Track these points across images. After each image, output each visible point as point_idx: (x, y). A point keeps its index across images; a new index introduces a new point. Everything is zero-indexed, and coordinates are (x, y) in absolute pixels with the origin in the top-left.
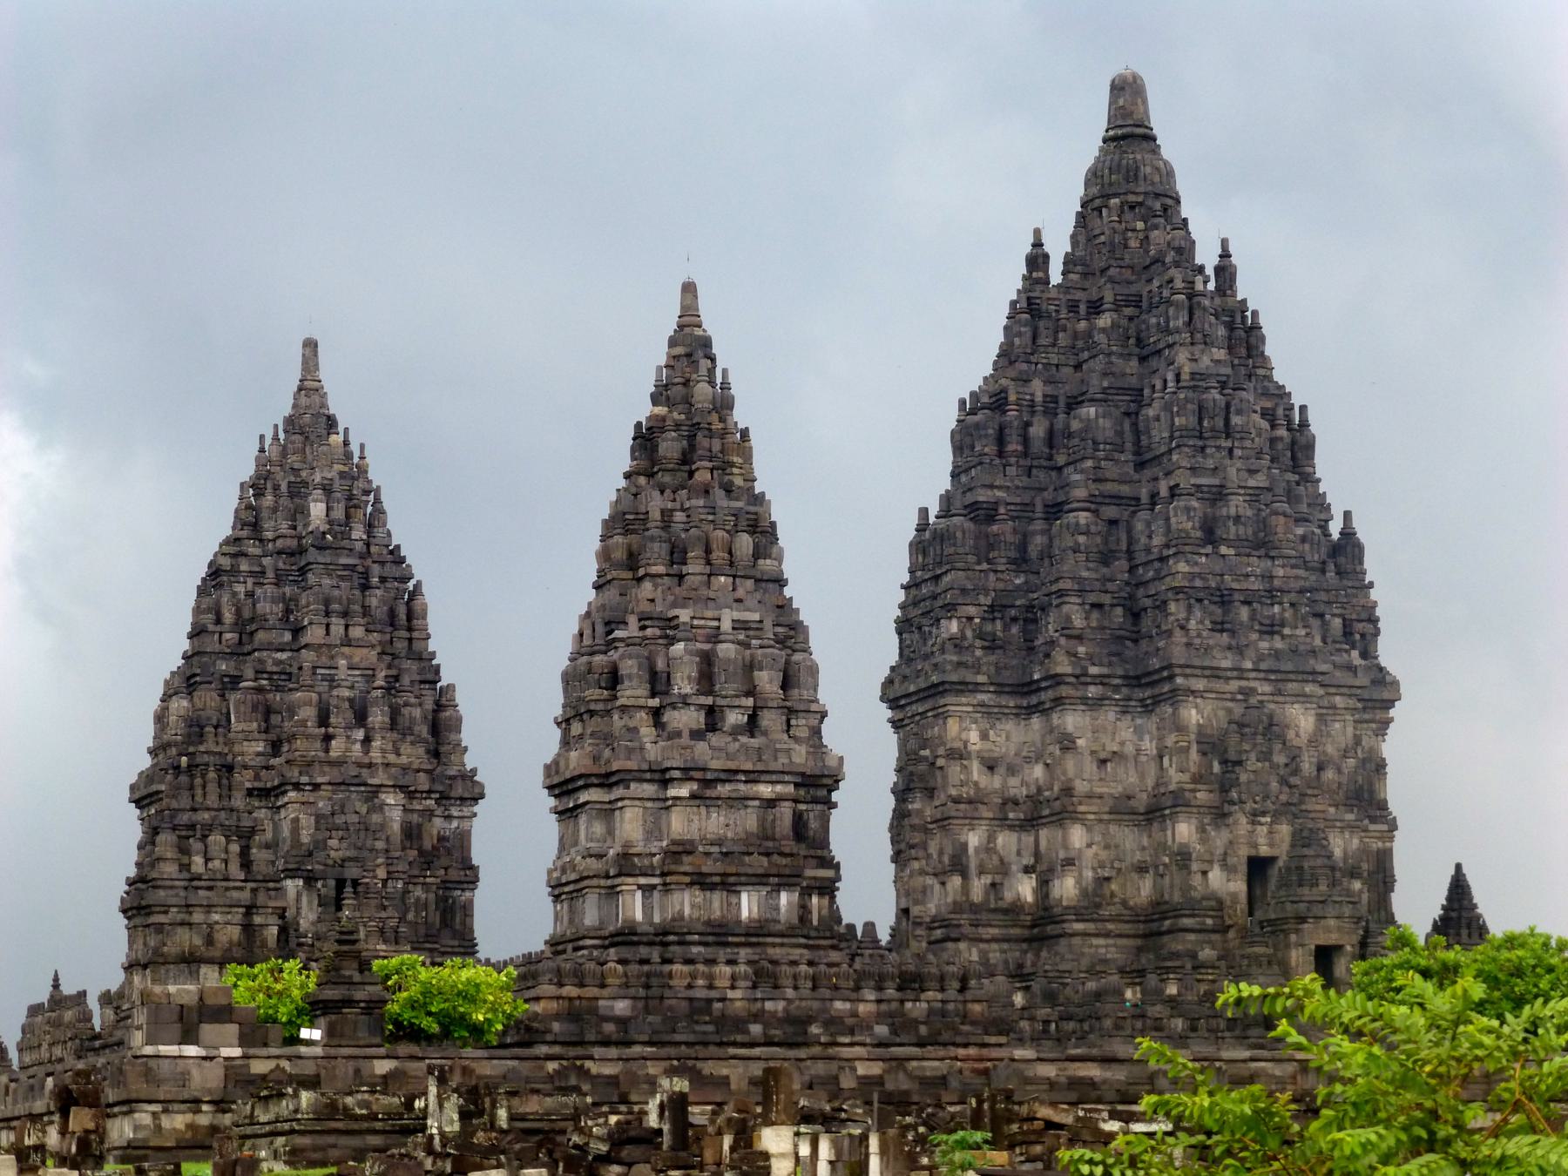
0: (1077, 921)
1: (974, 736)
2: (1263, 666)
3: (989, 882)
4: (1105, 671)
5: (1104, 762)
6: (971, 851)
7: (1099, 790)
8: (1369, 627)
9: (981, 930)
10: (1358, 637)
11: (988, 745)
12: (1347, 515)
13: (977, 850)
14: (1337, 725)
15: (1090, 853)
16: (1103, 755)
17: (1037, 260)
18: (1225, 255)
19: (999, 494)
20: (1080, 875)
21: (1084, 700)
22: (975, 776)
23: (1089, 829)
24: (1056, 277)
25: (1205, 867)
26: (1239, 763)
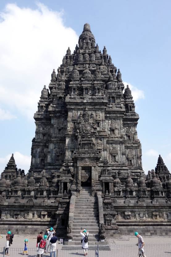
0: (49, 166)
1: (41, 129)
2: (89, 101)
3: (41, 159)
4: (60, 110)
5: (60, 130)
6: (38, 152)
7: (57, 136)
9: (37, 169)
10: (129, 107)
11: (44, 131)
13: (39, 152)
15: (55, 150)
16: (59, 128)
17: (69, 51)
18: (105, 48)
20: (52, 155)
21: (56, 117)
22: (41, 137)
23: (55, 145)
24: (72, 53)
25: (73, 150)
26: (80, 123)
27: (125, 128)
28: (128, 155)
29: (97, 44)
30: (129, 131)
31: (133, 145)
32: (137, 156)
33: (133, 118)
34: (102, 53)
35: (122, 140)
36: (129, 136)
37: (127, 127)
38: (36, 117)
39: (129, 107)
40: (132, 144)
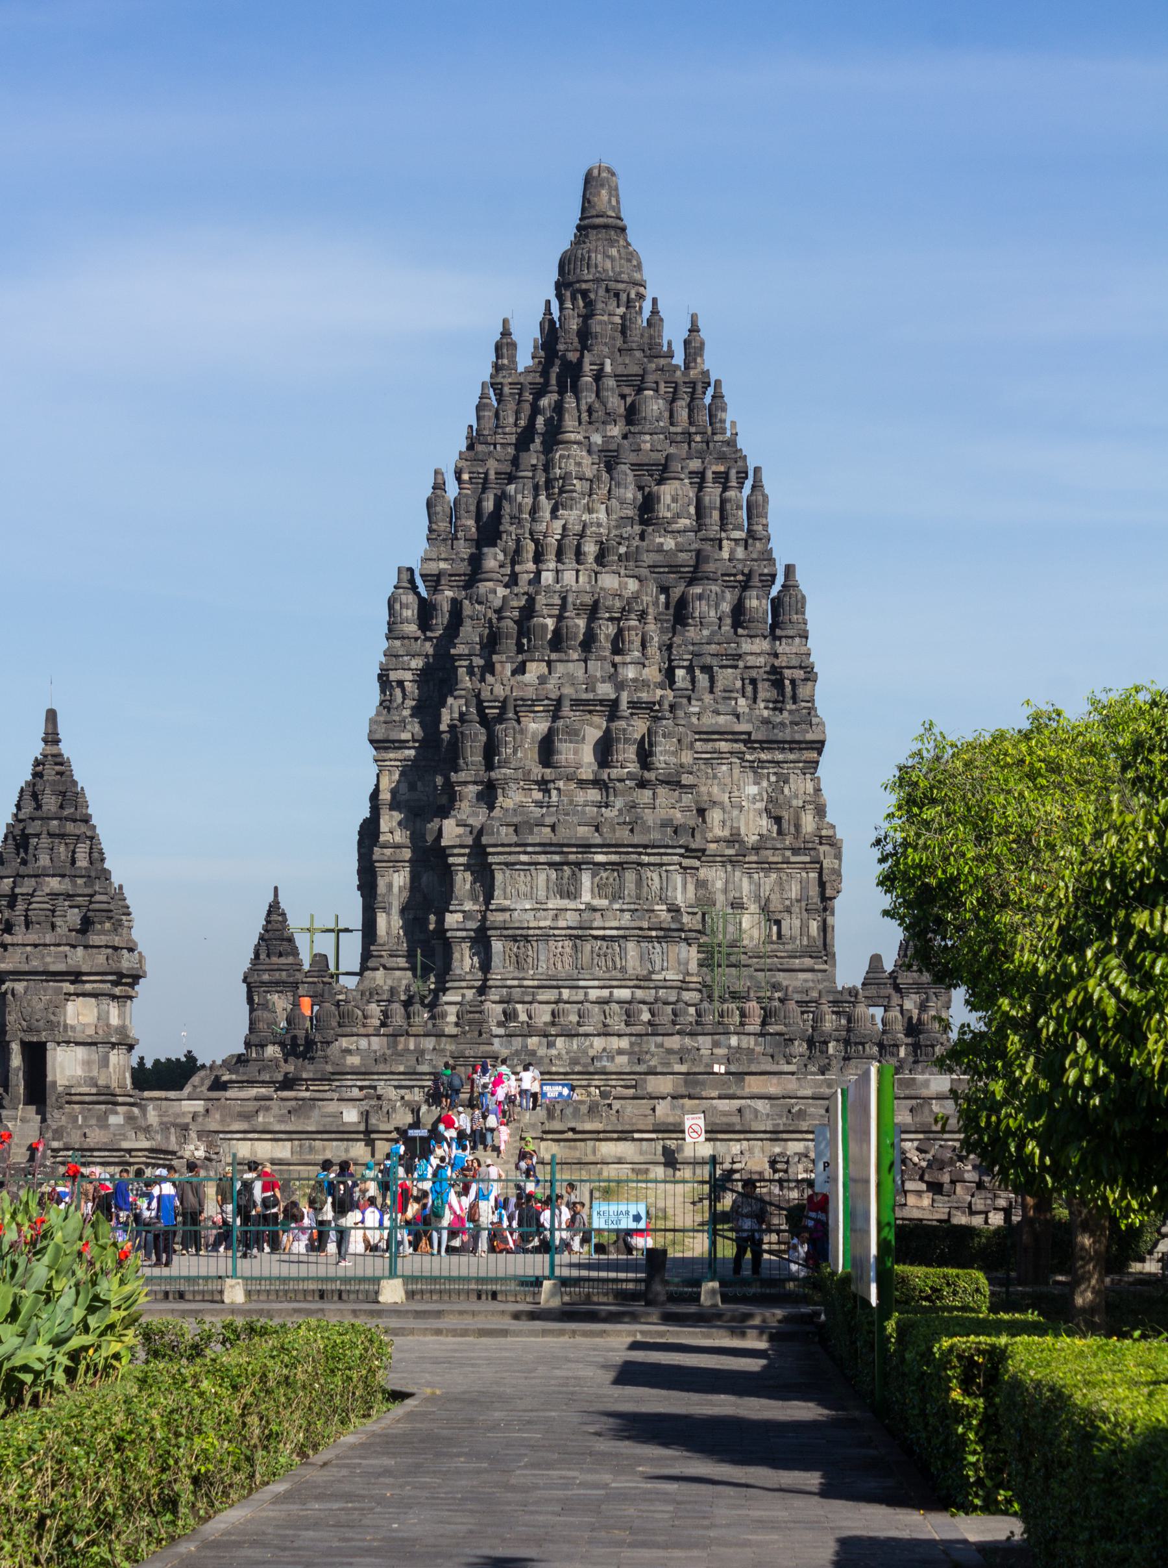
8: (799, 674)
12: (789, 570)
14: (724, 768)
17: (504, 346)
18: (694, 329)
19: (443, 565)
24: (525, 359)
27: (765, 784)
28: (768, 900)
29: (655, 301)
30: (781, 797)
31: (793, 859)
32: (803, 904)
33: (798, 737)
34: (679, 359)
35: (731, 852)
36: (778, 820)
37: (773, 778)
38: (378, 736)
39: (787, 682)
40: (788, 853)
